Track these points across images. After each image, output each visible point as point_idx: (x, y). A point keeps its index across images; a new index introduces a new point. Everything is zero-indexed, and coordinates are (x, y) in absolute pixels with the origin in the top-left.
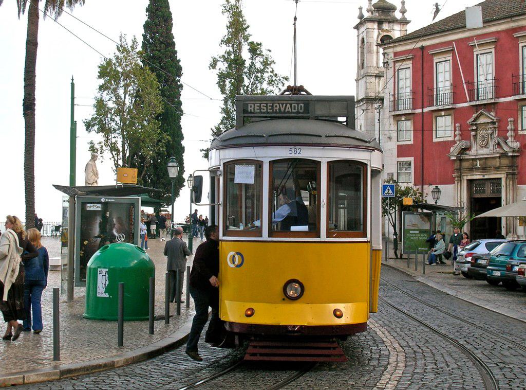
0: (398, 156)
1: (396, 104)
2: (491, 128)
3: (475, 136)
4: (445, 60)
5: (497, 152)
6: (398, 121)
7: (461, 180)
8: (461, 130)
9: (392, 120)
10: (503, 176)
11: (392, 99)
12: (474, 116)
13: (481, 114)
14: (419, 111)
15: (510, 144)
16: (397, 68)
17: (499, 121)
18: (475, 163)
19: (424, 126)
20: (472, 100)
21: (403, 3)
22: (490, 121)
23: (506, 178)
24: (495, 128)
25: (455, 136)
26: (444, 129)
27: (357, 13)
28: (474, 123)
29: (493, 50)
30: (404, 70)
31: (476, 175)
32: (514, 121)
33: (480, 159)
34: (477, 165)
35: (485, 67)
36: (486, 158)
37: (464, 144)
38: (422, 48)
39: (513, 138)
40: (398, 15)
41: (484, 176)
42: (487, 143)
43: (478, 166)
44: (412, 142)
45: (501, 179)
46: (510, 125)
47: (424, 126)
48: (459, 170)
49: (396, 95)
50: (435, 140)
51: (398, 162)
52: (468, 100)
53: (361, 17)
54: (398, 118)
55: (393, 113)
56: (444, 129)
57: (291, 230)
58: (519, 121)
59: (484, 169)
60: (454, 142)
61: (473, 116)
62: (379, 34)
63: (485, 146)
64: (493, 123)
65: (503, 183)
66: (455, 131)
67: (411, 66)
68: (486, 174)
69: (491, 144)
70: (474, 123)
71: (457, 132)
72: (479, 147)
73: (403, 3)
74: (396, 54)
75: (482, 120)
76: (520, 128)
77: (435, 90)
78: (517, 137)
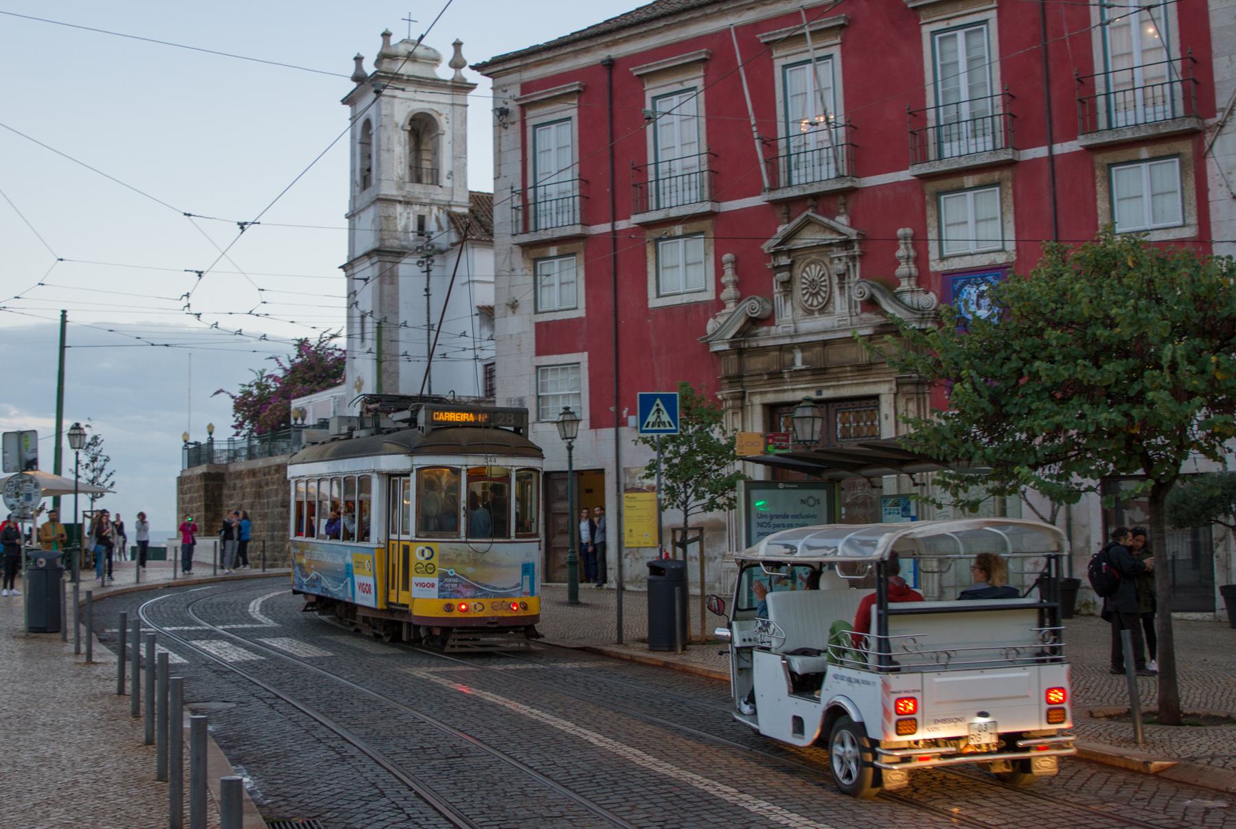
0: (539, 353)
1: (527, 211)
2: (839, 259)
3: (787, 285)
4: (679, 87)
5: (865, 325)
6: (535, 260)
7: (742, 408)
8: (736, 271)
10: (885, 390)
11: (518, 202)
12: (782, 229)
13: (808, 222)
14: (605, 228)
15: (907, 298)
16: (530, 123)
17: (863, 240)
18: (788, 357)
19: (615, 266)
20: (774, 187)
22: (836, 238)
23: (896, 394)
24: (853, 258)
25: (720, 287)
26: (683, 274)
27: (351, 69)
28: (785, 248)
29: (836, 52)
30: (553, 127)
31: (793, 390)
32: (913, 238)
33: (804, 347)
34: (794, 364)
36: (825, 343)
37: (753, 306)
38: (610, 64)
39: (913, 282)
41: (819, 393)
42: (829, 301)
43: (799, 365)
44: (581, 313)
45: (876, 397)
46: (902, 246)
47: (615, 266)
48: (736, 379)
49: (530, 193)
50: (653, 302)
51: (538, 367)
52: (766, 184)
53: (359, 78)
54: (535, 253)
55: (526, 238)
56: (683, 274)
57: (1122, 632)
58: (932, 234)
59: (818, 372)
60: (719, 304)
61: (780, 229)
63: (823, 310)
64: (846, 244)
65: (886, 407)
66: (719, 272)
67: (574, 113)
68: (828, 387)
69: (840, 304)
70: (785, 248)
71: (729, 276)
72: (801, 312)
74: (526, 87)
75: (809, 238)
76: (933, 254)
77: (651, 169)
78: (923, 279)
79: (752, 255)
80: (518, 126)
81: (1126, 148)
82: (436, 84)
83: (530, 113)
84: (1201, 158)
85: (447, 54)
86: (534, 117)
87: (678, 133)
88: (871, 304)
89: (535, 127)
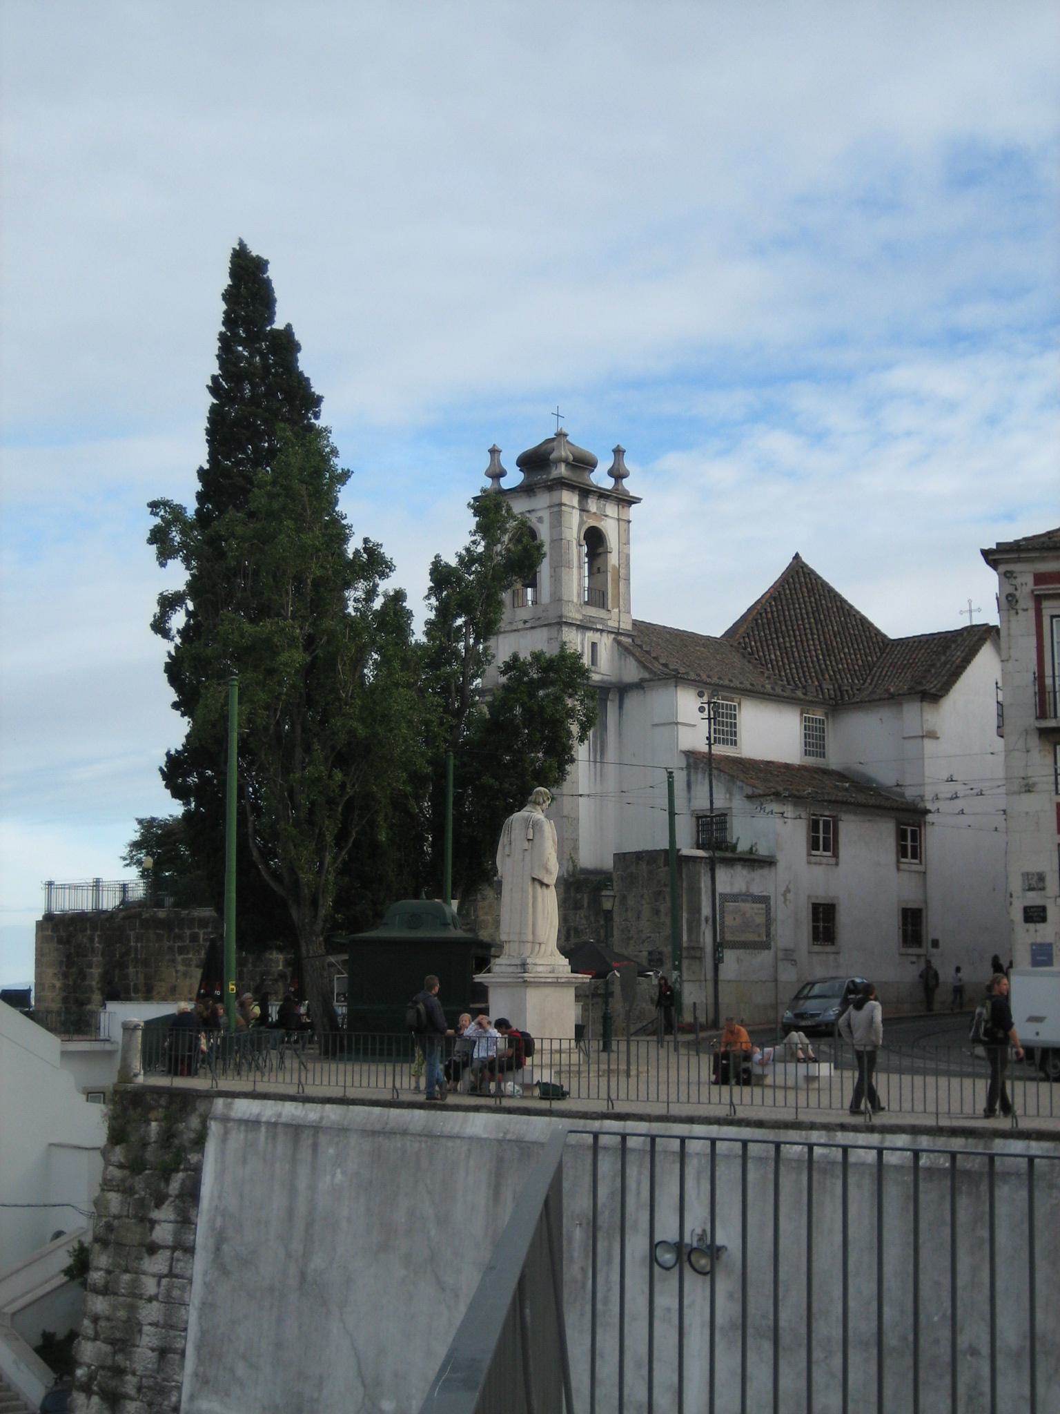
9: (1034, 741)
21: (618, 452)
40: (601, 478)
49: (1048, 681)
53: (497, 474)
62: (581, 523)
73: (618, 452)
74: (1040, 579)
80: (1032, 613)
82: (603, 495)
83: (1045, 604)
85: (604, 464)
86: (1049, 608)
89: (1052, 617)
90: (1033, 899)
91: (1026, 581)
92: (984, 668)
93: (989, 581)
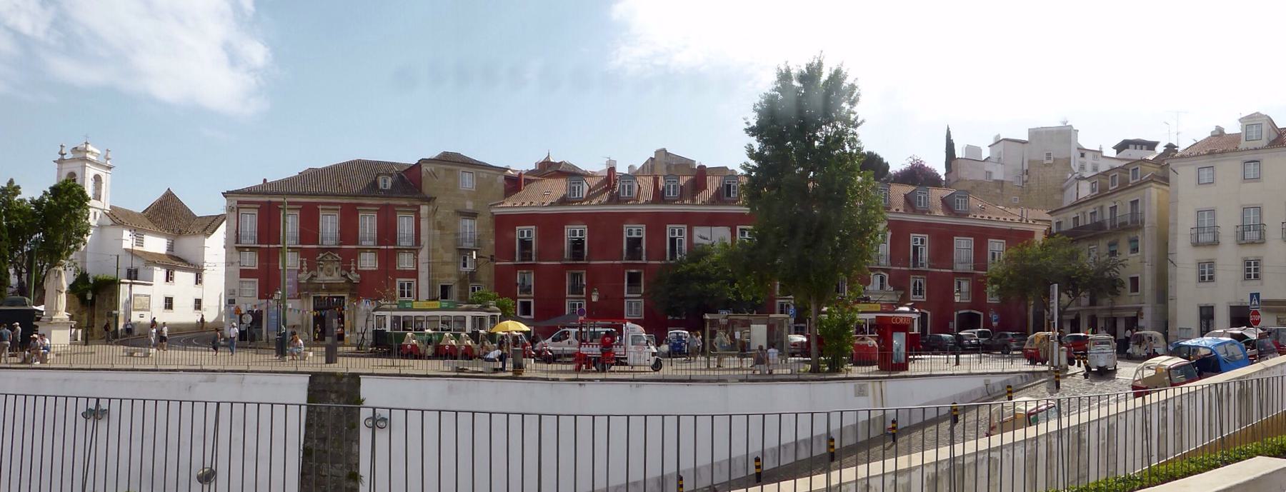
10: (346, 296)
26: (291, 261)
35: (329, 226)
56: (291, 261)
66: (302, 262)
69: (336, 274)
74: (239, 202)
78: (356, 271)
79: (311, 258)
81: (403, 250)
84: (417, 254)
87: (291, 225)
88: (345, 276)
90: (232, 297)
91: (234, 204)
92: (222, 228)
93: (224, 202)
